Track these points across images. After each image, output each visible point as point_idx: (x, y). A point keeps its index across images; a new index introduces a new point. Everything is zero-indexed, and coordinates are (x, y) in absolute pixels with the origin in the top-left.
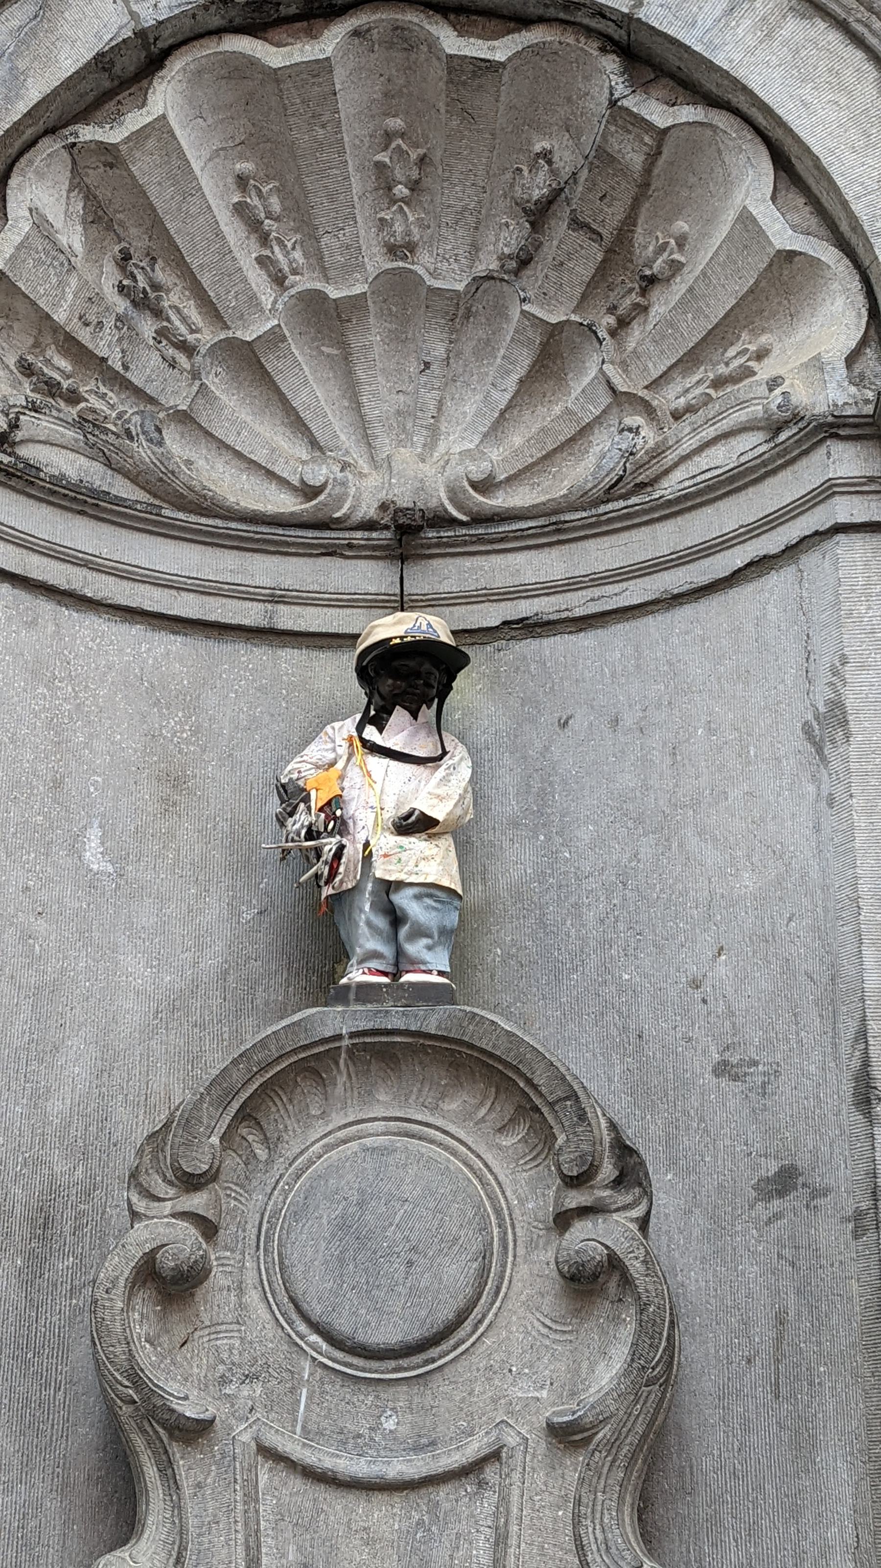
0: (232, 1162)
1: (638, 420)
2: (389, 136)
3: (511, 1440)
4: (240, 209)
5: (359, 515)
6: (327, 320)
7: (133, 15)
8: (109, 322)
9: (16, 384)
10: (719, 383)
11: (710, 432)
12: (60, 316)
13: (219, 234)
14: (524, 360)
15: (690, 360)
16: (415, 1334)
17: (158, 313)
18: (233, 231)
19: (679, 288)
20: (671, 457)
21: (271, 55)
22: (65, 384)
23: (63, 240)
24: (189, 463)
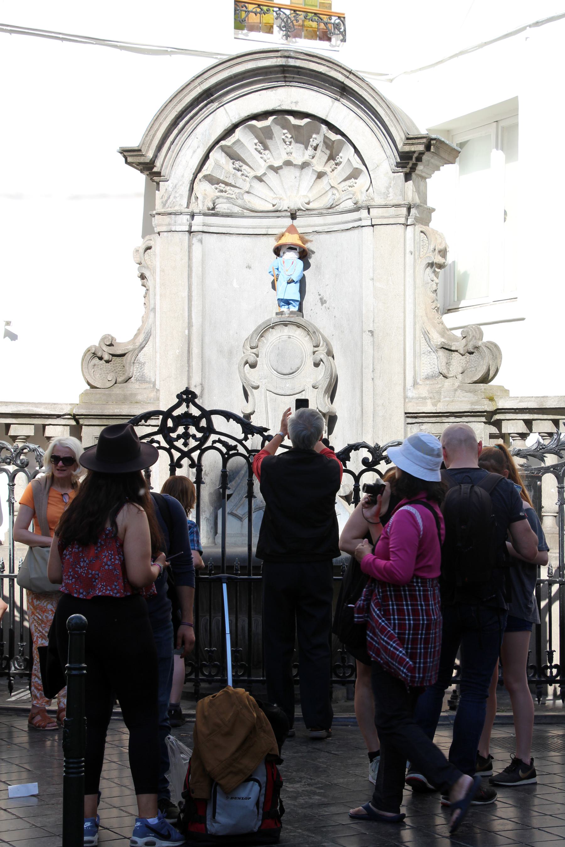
0: (260, 344)
1: (335, 192)
2: (284, 134)
3: (306, 387)
4: (256, 149)
5: (283, 209)
6: (275, 169)
7: (231, 120)
8: (231, 176)
9: (214, 192)
10: (349, 187)
11: (348, 197)
12: (221, 178)
13: (252, 155)
14: (315, 177)
15: (345, 180)
16: (291, 372)
17: (241, 171)
18: (255, 154)
19: (341, 166)
20: (341, 201)
21: (259, 124)
22: (224, 189)
23: (221, 162)
24: (249, 202)
